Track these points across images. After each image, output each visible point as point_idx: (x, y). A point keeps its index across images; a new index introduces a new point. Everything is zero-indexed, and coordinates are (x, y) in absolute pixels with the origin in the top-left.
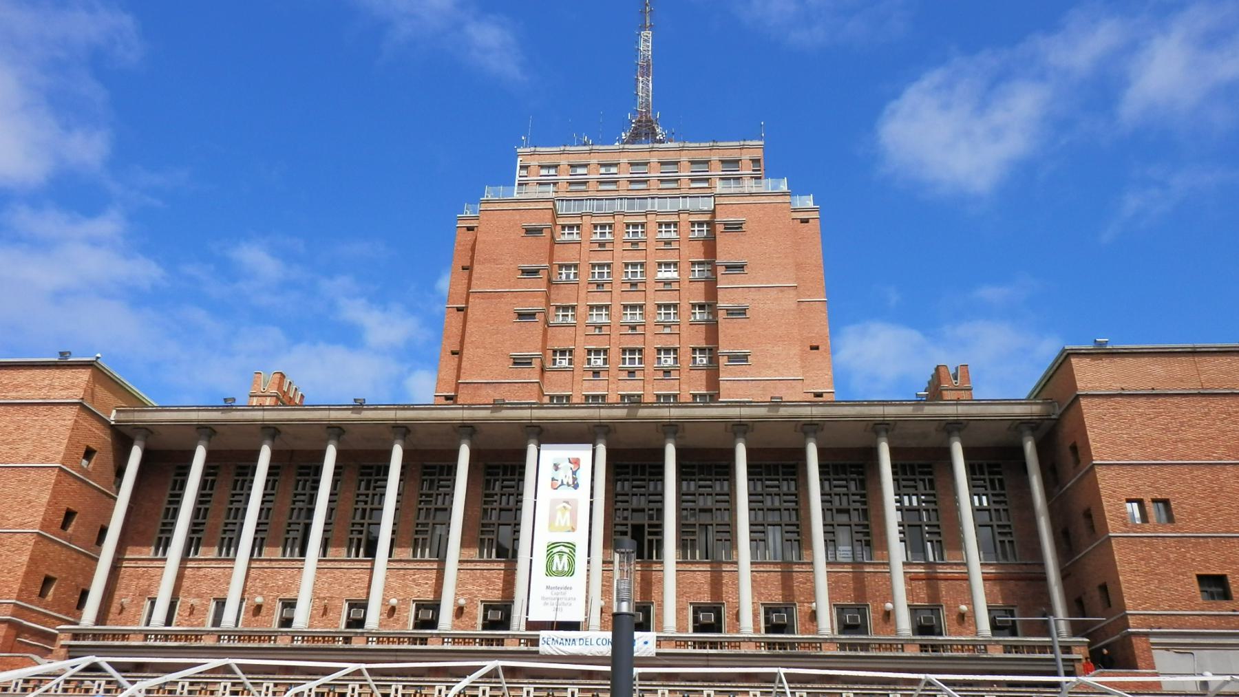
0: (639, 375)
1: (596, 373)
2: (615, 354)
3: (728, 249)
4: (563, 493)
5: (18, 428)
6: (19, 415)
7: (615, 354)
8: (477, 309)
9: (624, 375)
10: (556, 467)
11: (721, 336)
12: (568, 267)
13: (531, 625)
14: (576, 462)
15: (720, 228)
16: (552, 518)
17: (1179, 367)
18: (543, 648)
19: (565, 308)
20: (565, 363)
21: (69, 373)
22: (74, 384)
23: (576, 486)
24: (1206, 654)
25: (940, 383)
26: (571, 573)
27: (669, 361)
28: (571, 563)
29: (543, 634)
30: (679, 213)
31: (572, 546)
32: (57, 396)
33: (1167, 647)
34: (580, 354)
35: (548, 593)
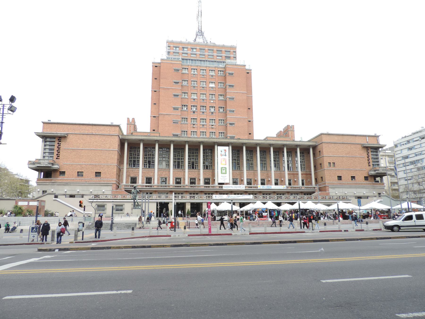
0: (205, 114)
1: (194, 112)
2: (199, 107)
3: (230, 81)
4: (223, 157)
5: (104, 141)
6: (104, 137)
7: (199, 107)
8: (162, 93)
9: (201, 113)
10: (221, 151)
11: (227, 105)
12: (185, 81)
13: (219, 184)
14: (225, 150)
15: (227, 74)
16: (221, 162)
17: (340, 138)
18: (224, 188)
19: (185, 93)
20: (185, 109)
21: (113, 128)
22: (115, 131)
23: (226, 156)
24: (337, 189)
25: (288, 129)
26: (226, 173)
27: (212, 110)
28: (226, 171)
29: (223, 185)
30: (215, 67)
31: (226, 168)
32: (112, 133)
33: (331, 188)
34: (189, 107)
35: (222, 177)
